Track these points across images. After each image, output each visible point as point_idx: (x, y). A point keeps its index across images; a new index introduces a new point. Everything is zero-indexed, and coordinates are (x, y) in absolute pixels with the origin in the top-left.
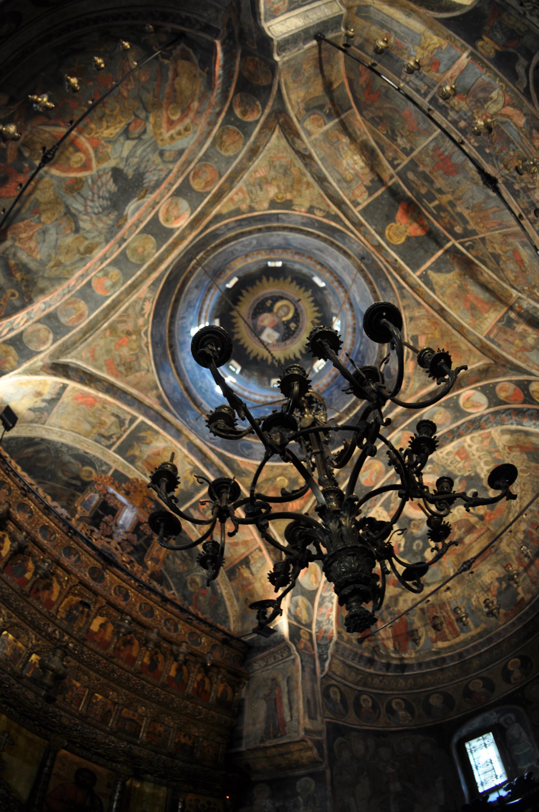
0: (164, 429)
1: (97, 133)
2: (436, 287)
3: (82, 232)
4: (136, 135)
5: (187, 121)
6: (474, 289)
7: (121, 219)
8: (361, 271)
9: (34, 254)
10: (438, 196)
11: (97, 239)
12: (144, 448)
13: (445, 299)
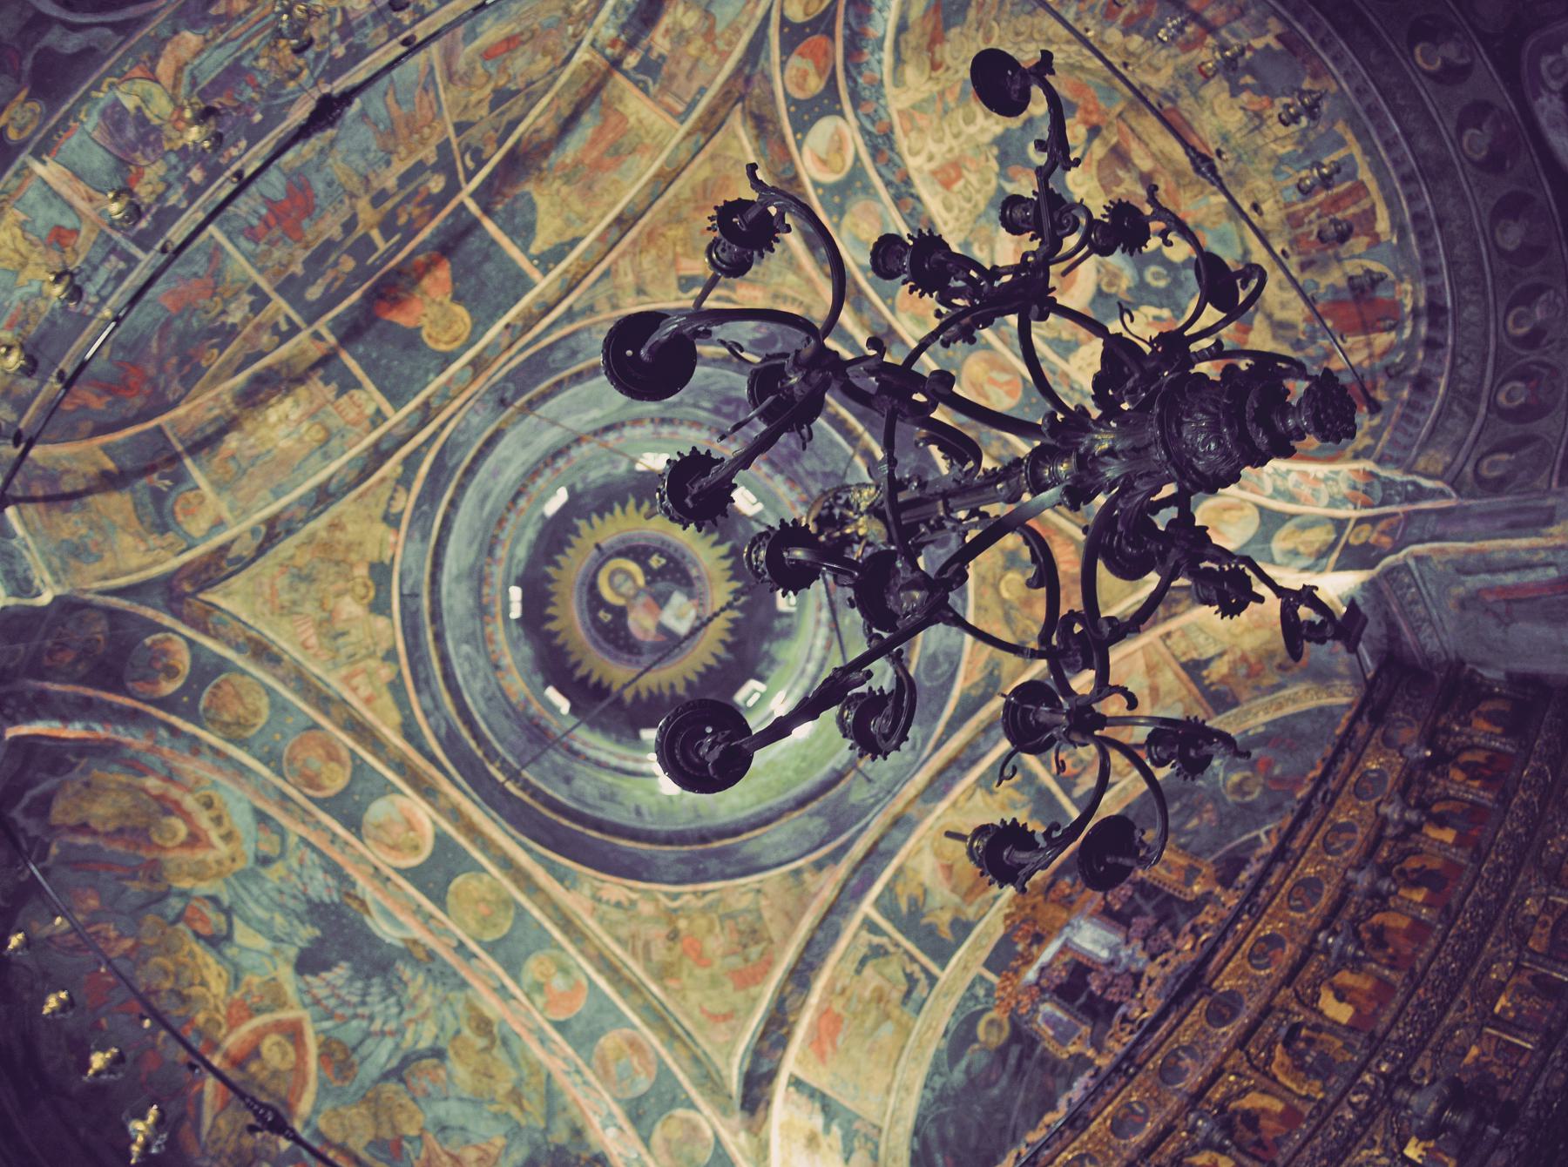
1: (217, 1009)
2: (568, 237)
3: (442, 1043)
4: (223, 918)
5: (189, 802)
7: (411, 952)
8: (531, 405)
9: (493, 1151)
10: (359, 231)
11: (460, 1008)
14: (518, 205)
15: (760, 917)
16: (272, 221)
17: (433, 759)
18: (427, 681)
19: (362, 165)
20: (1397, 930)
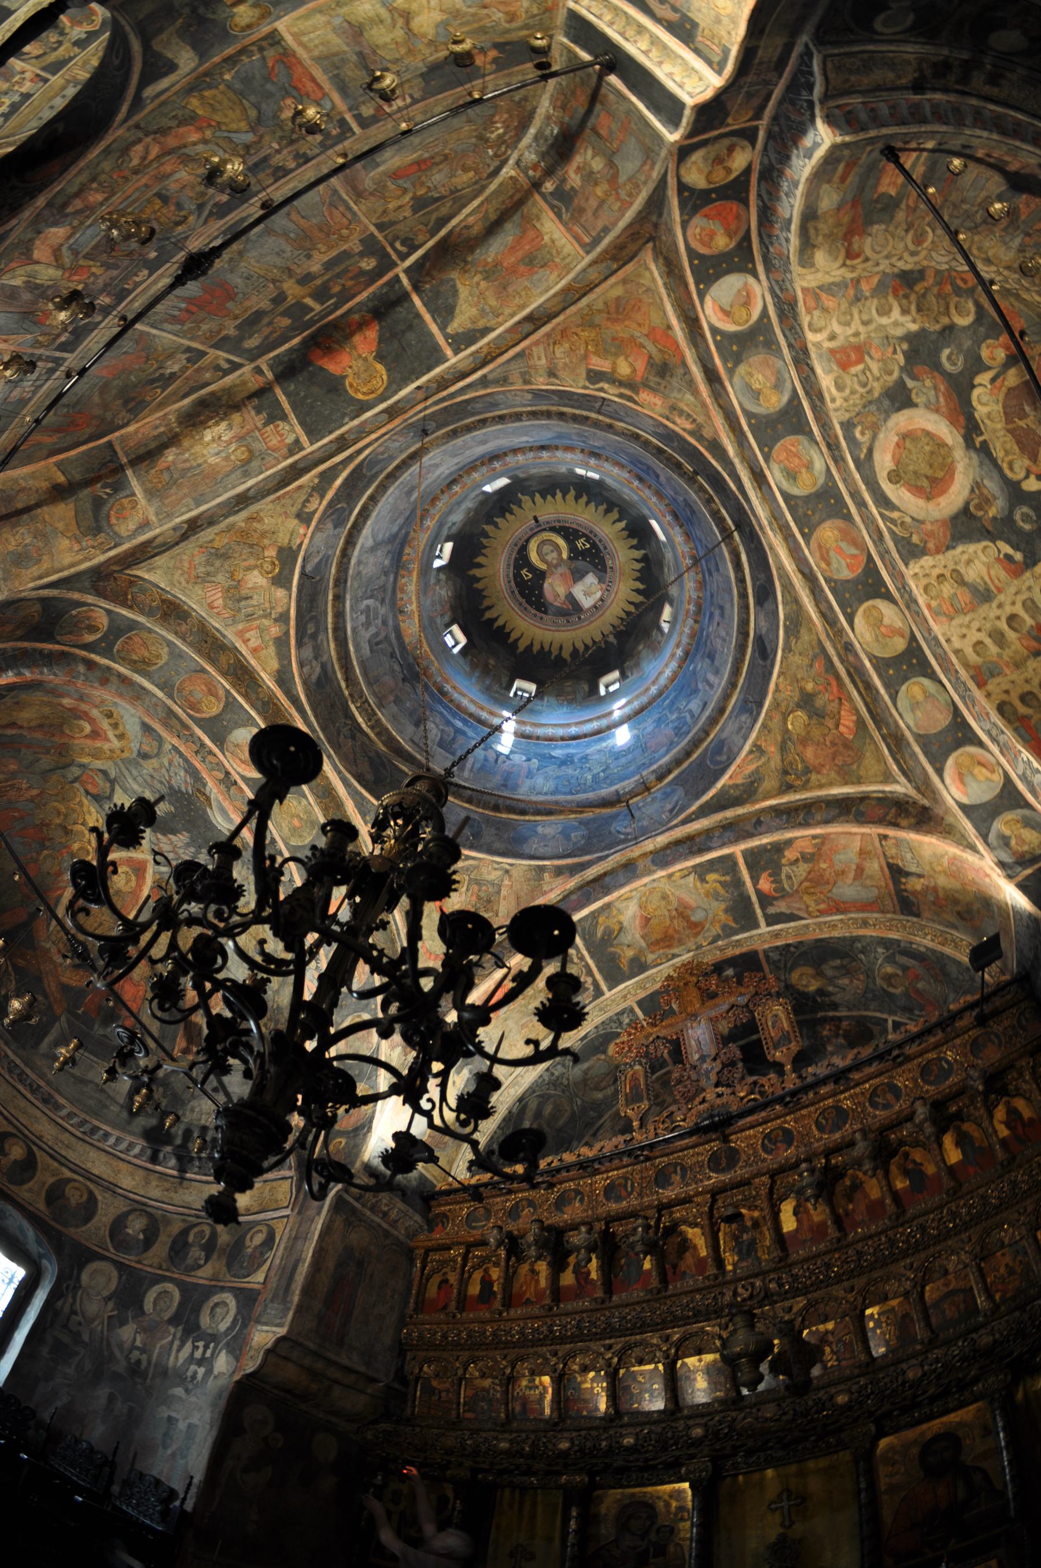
0: (607, 891)
2: (481, 324)
6: (495, 250)
8: (455, 434)
12: (625, 938)
13: (507, 311)
14: (443, 289)
15: (499, 892)
16: (194, 309)
17: (295, 701)
18: (314, 636)
19: (278, 261)
20: (866, 1196)
